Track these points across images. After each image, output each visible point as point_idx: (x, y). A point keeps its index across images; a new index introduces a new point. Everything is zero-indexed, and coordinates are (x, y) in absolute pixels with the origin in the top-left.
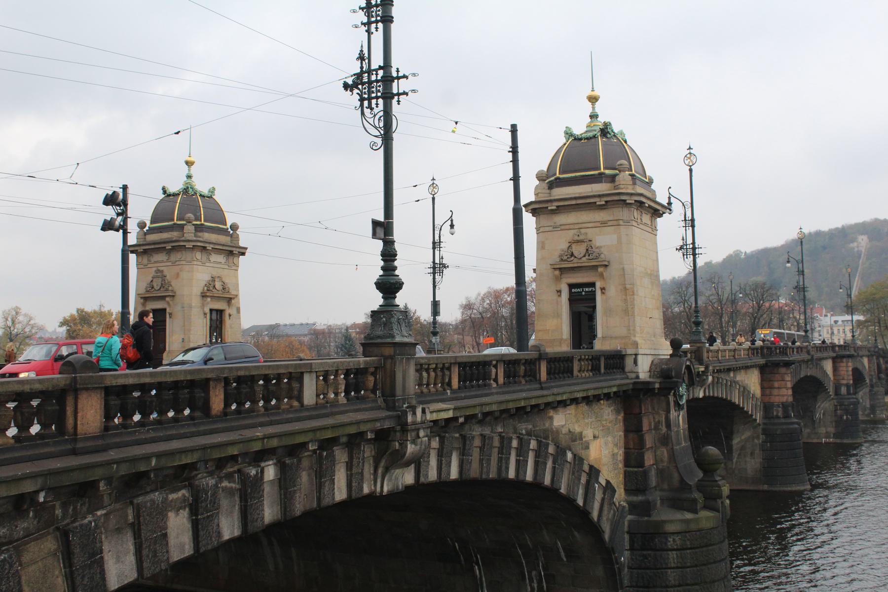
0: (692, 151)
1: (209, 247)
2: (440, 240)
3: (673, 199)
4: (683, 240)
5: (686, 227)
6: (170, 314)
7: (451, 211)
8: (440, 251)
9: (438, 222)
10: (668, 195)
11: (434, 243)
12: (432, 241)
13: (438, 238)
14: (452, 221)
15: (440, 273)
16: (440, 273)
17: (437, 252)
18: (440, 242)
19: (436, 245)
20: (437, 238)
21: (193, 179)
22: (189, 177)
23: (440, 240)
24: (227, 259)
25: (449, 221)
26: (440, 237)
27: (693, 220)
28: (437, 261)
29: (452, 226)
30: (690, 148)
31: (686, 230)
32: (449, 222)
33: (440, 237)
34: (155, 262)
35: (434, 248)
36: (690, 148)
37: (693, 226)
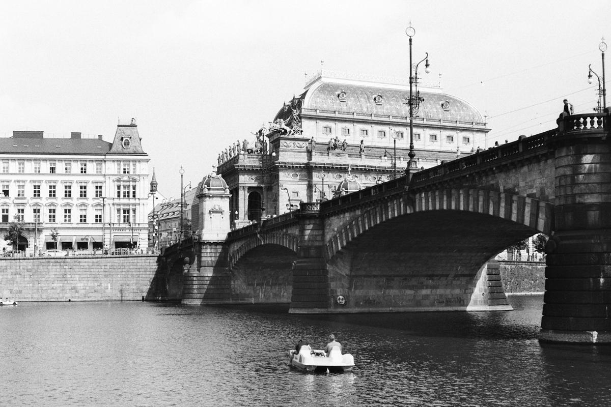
2: (416, 76)
3: (592, 74)
4: (598, 103)
5: (600, 94)
8: (416, 86)
9: (415, 61)
10: (589, 70)
11: (411, 78)
13: (415, 75)
14: (427, 61)
15: (416, 104)
16: (416, 104)
18: (416, 78)
20: (413, 75)
23: (416, 76)
27: (604, 90)
29: (427, 65)
31: (600, 97)
32: (425, 62)
35: (411, 83)
37: (604, 95)
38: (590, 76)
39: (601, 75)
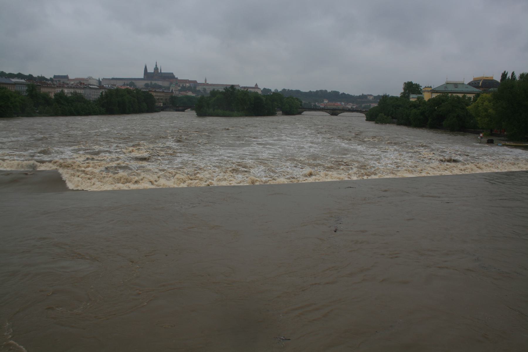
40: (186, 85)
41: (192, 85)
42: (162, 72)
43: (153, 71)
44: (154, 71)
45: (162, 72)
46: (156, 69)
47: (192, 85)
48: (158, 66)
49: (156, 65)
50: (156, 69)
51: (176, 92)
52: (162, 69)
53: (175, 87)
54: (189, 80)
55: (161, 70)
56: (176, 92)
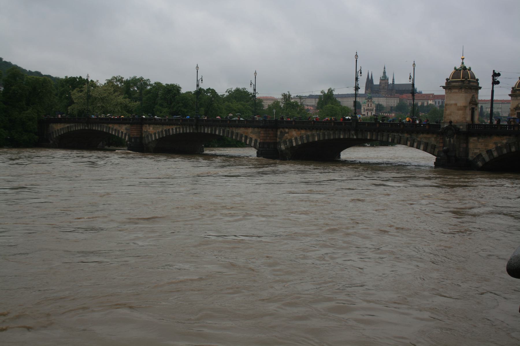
0: (415, 63)
1: (472, 88)
6: (476, 109)
7: (361, 67)
9: (358, 70)
10: (410, 76)
12: (355, 77)
14: (361, 71)
17: (357, 82)
18: (358, 78)
19: (357, 79)
21: (464, 64)
22: (463, 63)
24: (459, 91)
25: (360, 71)
26: (358, 76)
28: (357, 85)
29: (361, 73)
30: (414, 62)
32: (360, 72)
33: (358, 76)
34: (473, 92)
35: (356, 80)
36: (414, 62)
38: (410, 79)
39: (413, 78)
40: (428, 103)
41: (439, 104)
42: (395, 83)
43: (378, 83)
44: (380, 82)
45: (395, 83)
46: (384, 78)
47: (439, 102)
48: (387, 74)
49: (384, 73)
50: (384, 78)
51: (367, 113)
52: (394, 78)
53: (367, 105)
54: (435, 94)
55: (393, 79)
56: (367, 113)
